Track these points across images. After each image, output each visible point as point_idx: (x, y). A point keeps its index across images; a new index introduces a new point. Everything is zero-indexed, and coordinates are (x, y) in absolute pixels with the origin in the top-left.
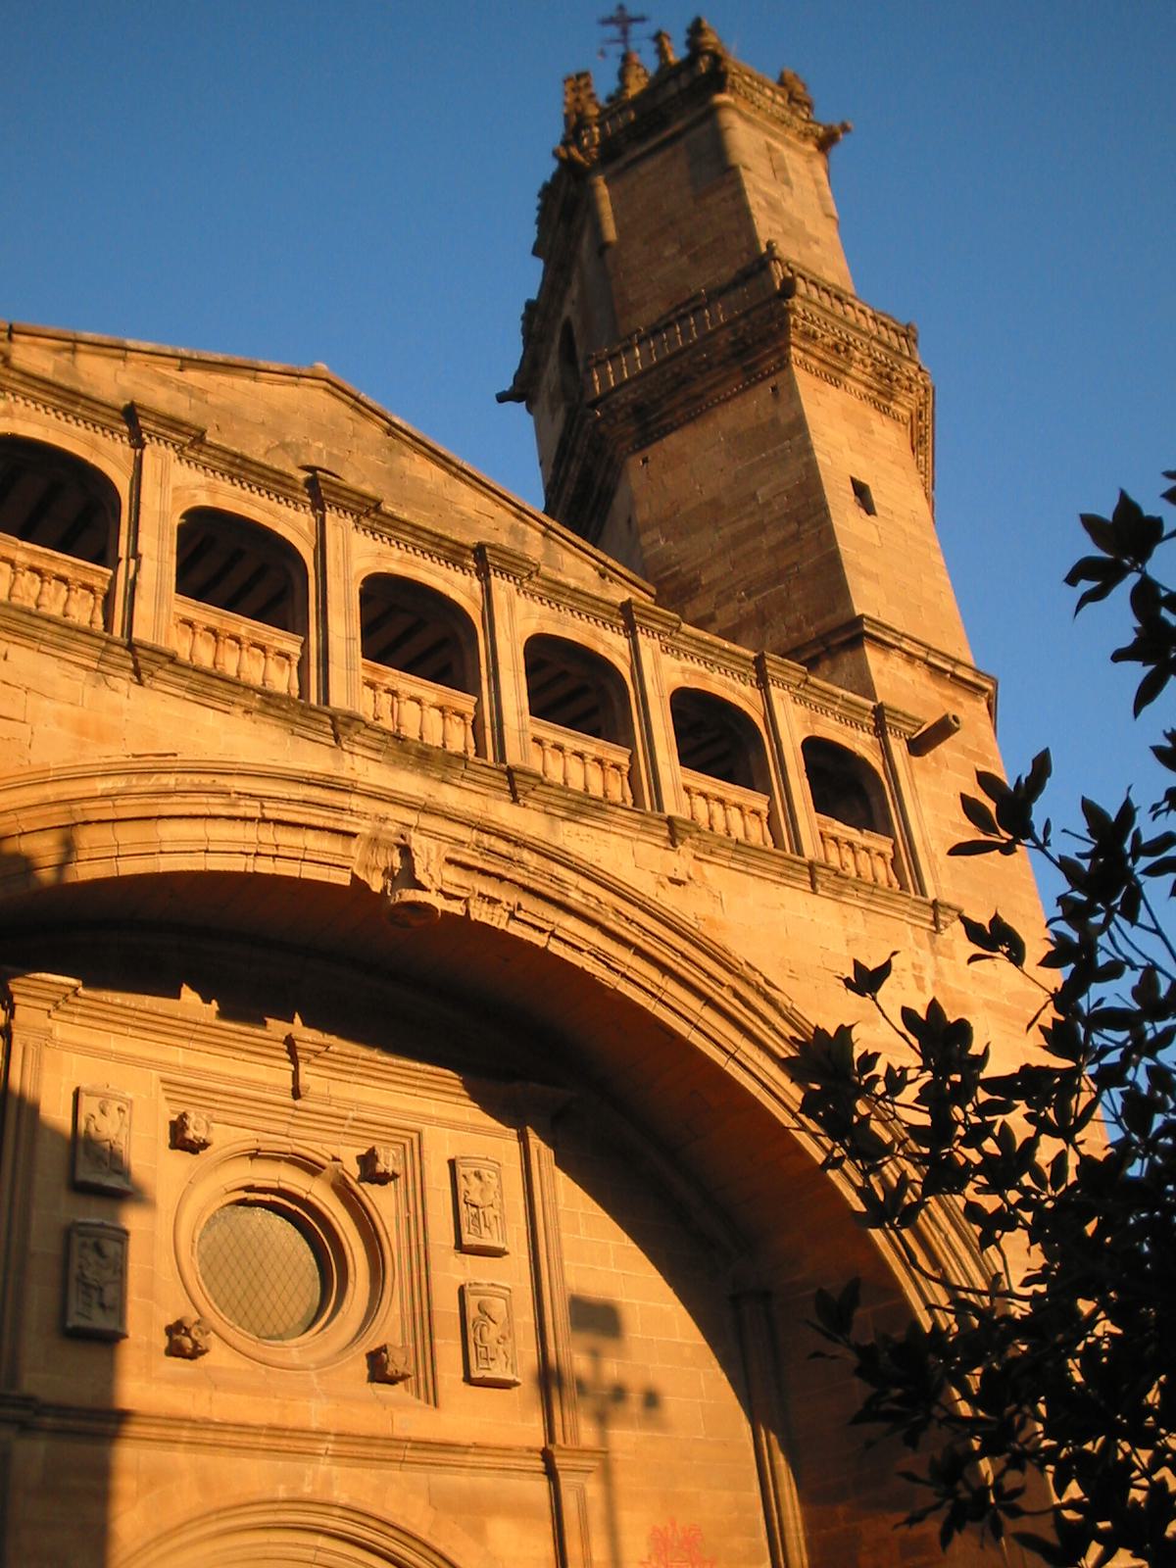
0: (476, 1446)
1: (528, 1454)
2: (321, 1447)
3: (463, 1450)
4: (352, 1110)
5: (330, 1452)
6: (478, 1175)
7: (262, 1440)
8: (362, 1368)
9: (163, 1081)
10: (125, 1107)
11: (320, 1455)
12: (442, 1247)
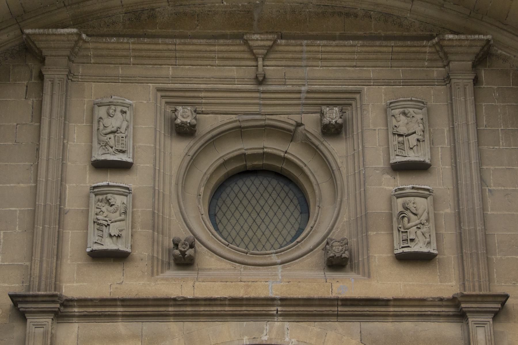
0: (395, 300)
1: (440, 303)
2: (273, 310)
3: (383, 303)
4: (304, 85)
5: (279, 313)
6: (404, 114)
7: (227, 309)
8: (317, 257)
9: (159, 90)
10: (125, 109)
11: (273, 315)
12: (376, 169)
